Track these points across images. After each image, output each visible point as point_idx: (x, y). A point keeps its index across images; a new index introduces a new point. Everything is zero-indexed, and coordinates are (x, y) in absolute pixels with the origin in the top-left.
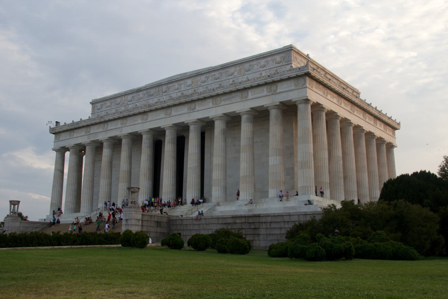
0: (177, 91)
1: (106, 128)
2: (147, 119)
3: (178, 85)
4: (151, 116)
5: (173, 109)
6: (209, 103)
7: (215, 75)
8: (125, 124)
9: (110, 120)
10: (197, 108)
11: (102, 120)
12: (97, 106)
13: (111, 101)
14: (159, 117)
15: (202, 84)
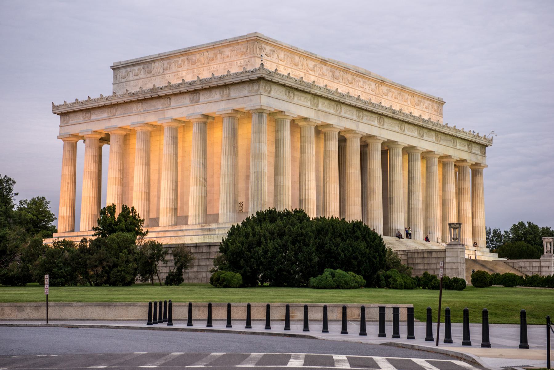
0: (362, 89)
1: (340, 113)
2: (383, 125)
3: (364, 82)
4: (388, 123)
5: (407, 126)
6: (432, 137)
7: (394, 93)
8: (362, 119)
9: (350, 105)
10: (425, 137)
11: (342, 100)
12: (265, 49)
13: (286, 53)
14: (394, 129)
15: (384, 97)
